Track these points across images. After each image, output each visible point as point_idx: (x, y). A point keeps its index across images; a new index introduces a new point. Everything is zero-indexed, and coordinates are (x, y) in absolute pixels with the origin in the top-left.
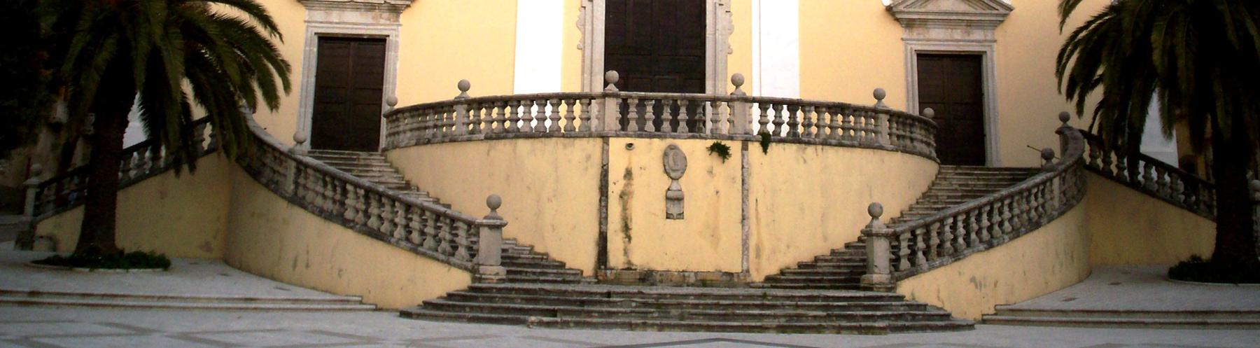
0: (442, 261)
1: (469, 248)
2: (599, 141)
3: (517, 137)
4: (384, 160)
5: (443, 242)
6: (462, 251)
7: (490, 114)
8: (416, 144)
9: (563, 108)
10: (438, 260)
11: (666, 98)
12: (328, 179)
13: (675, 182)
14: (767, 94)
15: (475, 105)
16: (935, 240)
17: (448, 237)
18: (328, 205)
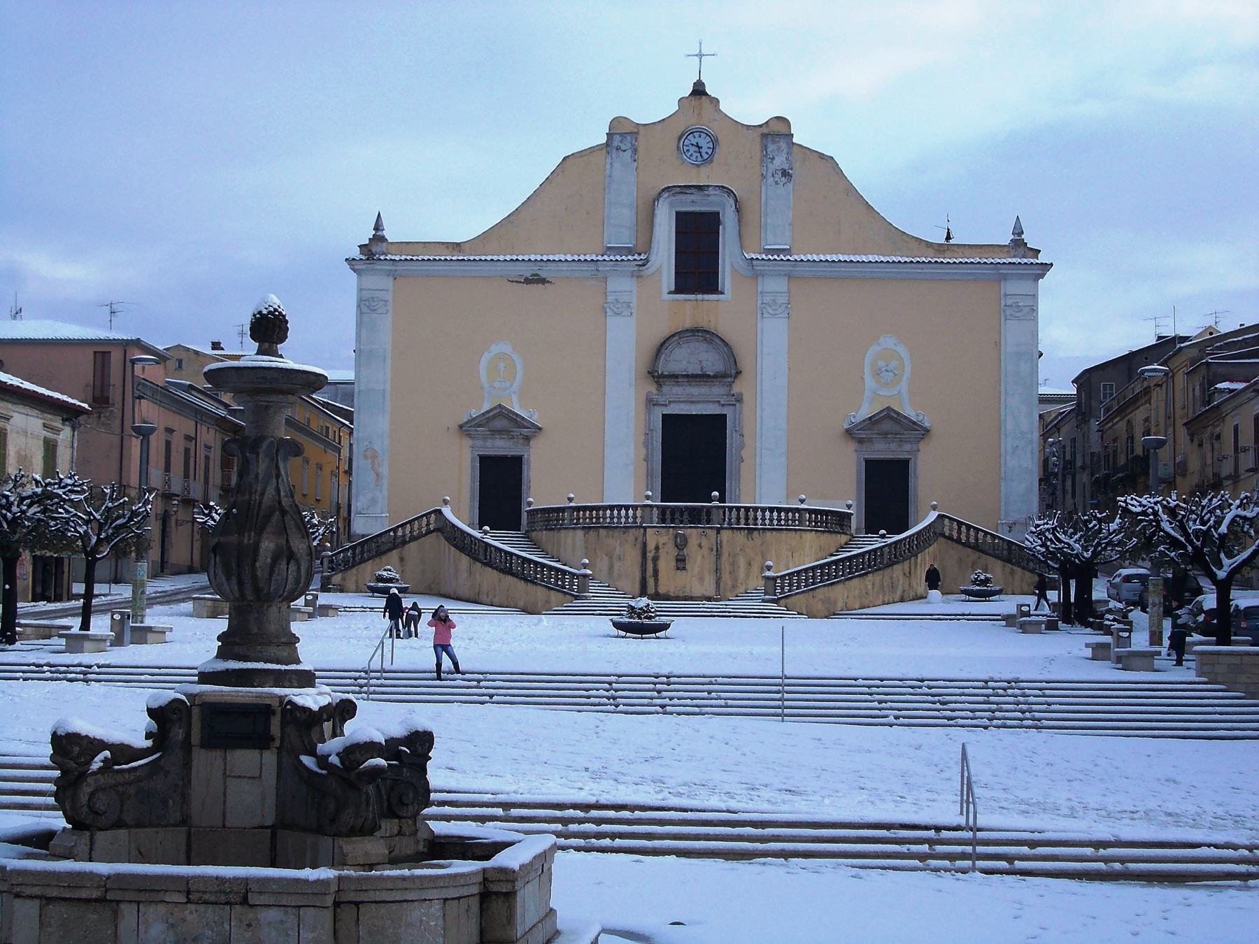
9: (623, 512)
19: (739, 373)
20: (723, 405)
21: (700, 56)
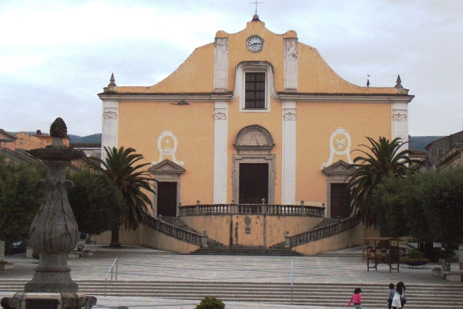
1: (200, 241)
2: (230, 216)
6: (198, 242)
8: (187, 216)
17: (195, 238)
18: (168, 232)
19: (274, 145)
20: (267, 159)
21: (257, 3)
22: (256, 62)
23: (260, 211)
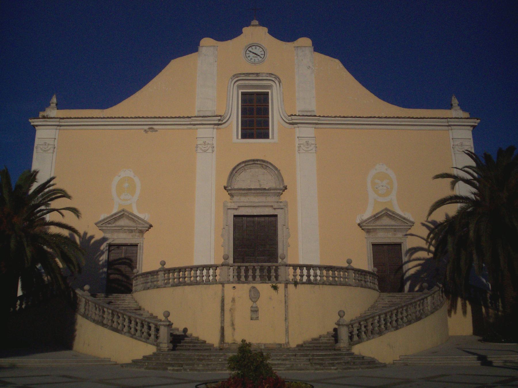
0: (144, 342)
2: (221, 285)
3: (185, 285)
4: (132, 297)
5: (144, 333)
7: (174, 275)
8: (144, 290)
10: (142, 341)
11: (250, 265)
12: (97, 306)
13: (255, 304)
14: (301, 263)
15: (167, 272)
16: (370, 327)
18: (97, 318)
20: (275, 209)
22: (257, 74)
23: (277, 277)
